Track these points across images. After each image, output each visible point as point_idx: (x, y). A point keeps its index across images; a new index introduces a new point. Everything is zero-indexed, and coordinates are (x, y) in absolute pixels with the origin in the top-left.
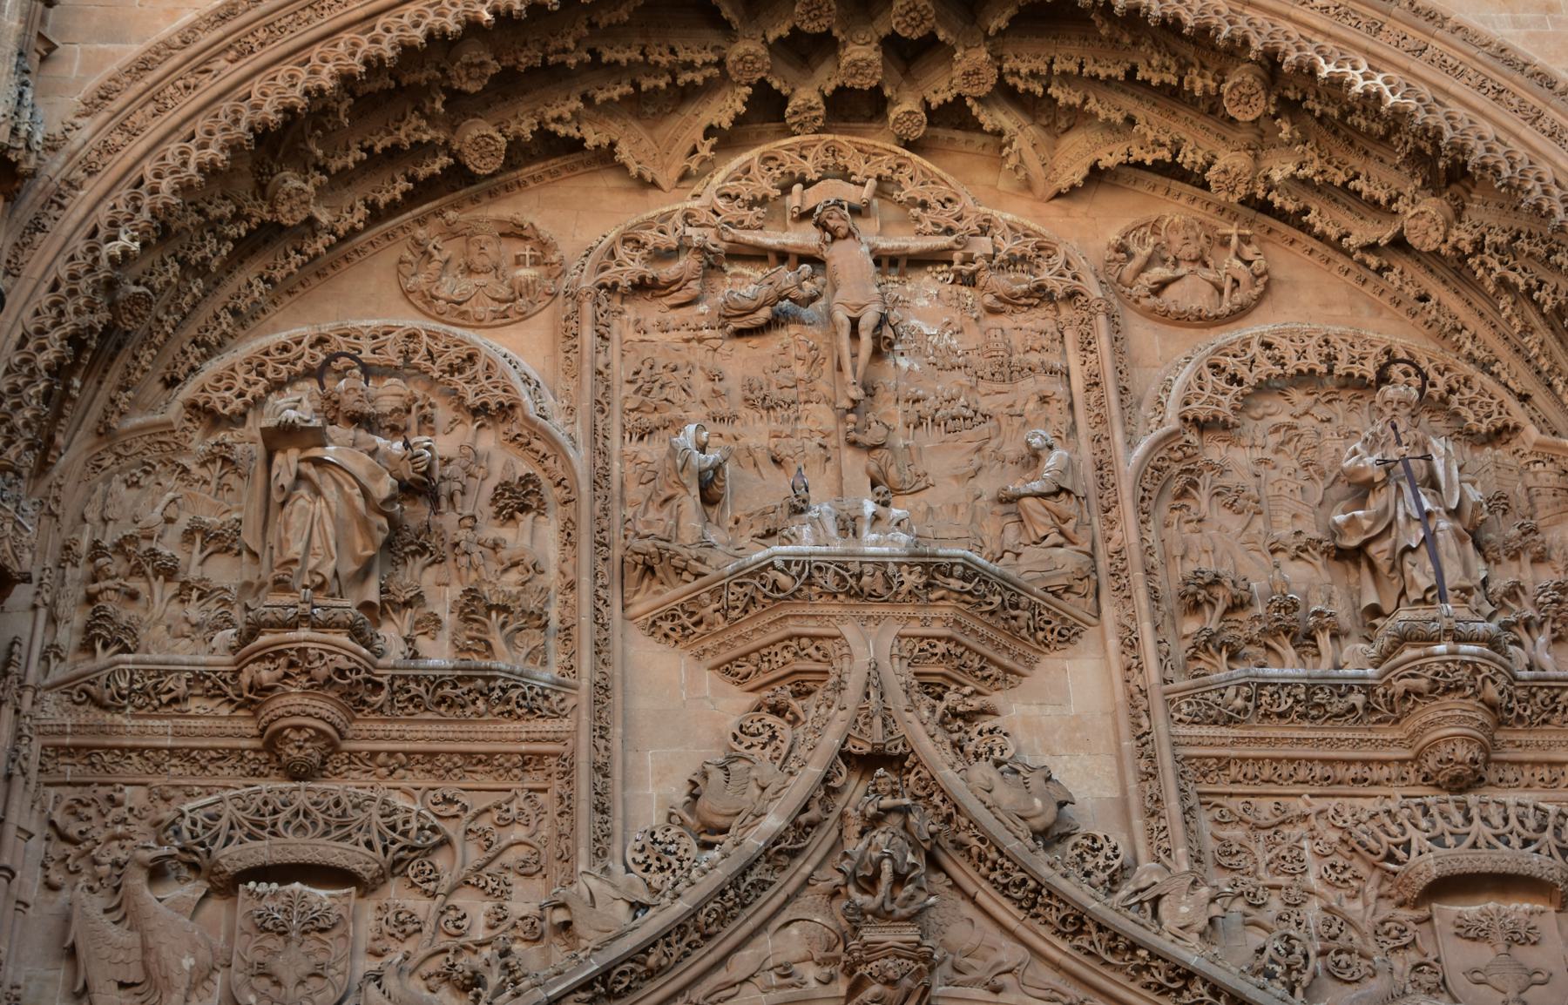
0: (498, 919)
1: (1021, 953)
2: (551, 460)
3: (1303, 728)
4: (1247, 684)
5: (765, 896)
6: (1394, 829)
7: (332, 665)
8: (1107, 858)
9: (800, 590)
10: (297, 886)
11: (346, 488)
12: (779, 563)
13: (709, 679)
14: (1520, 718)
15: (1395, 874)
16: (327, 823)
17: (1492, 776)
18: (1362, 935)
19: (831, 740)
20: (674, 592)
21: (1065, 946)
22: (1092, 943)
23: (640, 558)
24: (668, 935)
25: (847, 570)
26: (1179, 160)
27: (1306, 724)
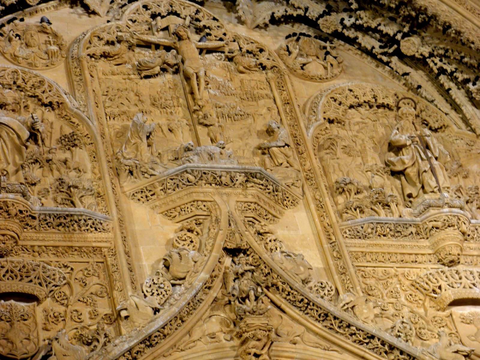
0: (94, 315)
1: (303, 328)
2: (81, 126)
3: (393, 241)
4: (372, 223)
5: (202, 305)
6: (434, 281)
7: (18, 209)
8: (328, 291)
9: (197, 182)
10: (12, 302)
11: (11, 134)
12: (189, 170)
13: (159, 218)
14: (473, 238)
15: (435, 298)
16: (21, 276)
17: (462, 260)
18: (427, 322)
19: (220, 243)
20: (142, 182)
21: (319, 325)
22: (332, 324)
23: (127, 168)
24: (171, 321)
25: (216, 174)
26: (307, 15)
27: (394, 239)
